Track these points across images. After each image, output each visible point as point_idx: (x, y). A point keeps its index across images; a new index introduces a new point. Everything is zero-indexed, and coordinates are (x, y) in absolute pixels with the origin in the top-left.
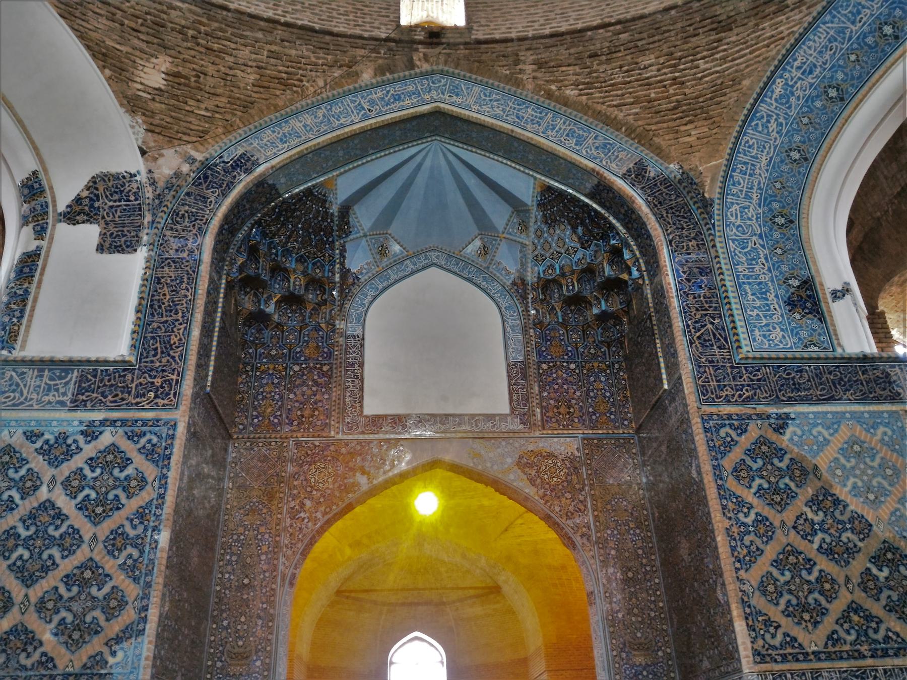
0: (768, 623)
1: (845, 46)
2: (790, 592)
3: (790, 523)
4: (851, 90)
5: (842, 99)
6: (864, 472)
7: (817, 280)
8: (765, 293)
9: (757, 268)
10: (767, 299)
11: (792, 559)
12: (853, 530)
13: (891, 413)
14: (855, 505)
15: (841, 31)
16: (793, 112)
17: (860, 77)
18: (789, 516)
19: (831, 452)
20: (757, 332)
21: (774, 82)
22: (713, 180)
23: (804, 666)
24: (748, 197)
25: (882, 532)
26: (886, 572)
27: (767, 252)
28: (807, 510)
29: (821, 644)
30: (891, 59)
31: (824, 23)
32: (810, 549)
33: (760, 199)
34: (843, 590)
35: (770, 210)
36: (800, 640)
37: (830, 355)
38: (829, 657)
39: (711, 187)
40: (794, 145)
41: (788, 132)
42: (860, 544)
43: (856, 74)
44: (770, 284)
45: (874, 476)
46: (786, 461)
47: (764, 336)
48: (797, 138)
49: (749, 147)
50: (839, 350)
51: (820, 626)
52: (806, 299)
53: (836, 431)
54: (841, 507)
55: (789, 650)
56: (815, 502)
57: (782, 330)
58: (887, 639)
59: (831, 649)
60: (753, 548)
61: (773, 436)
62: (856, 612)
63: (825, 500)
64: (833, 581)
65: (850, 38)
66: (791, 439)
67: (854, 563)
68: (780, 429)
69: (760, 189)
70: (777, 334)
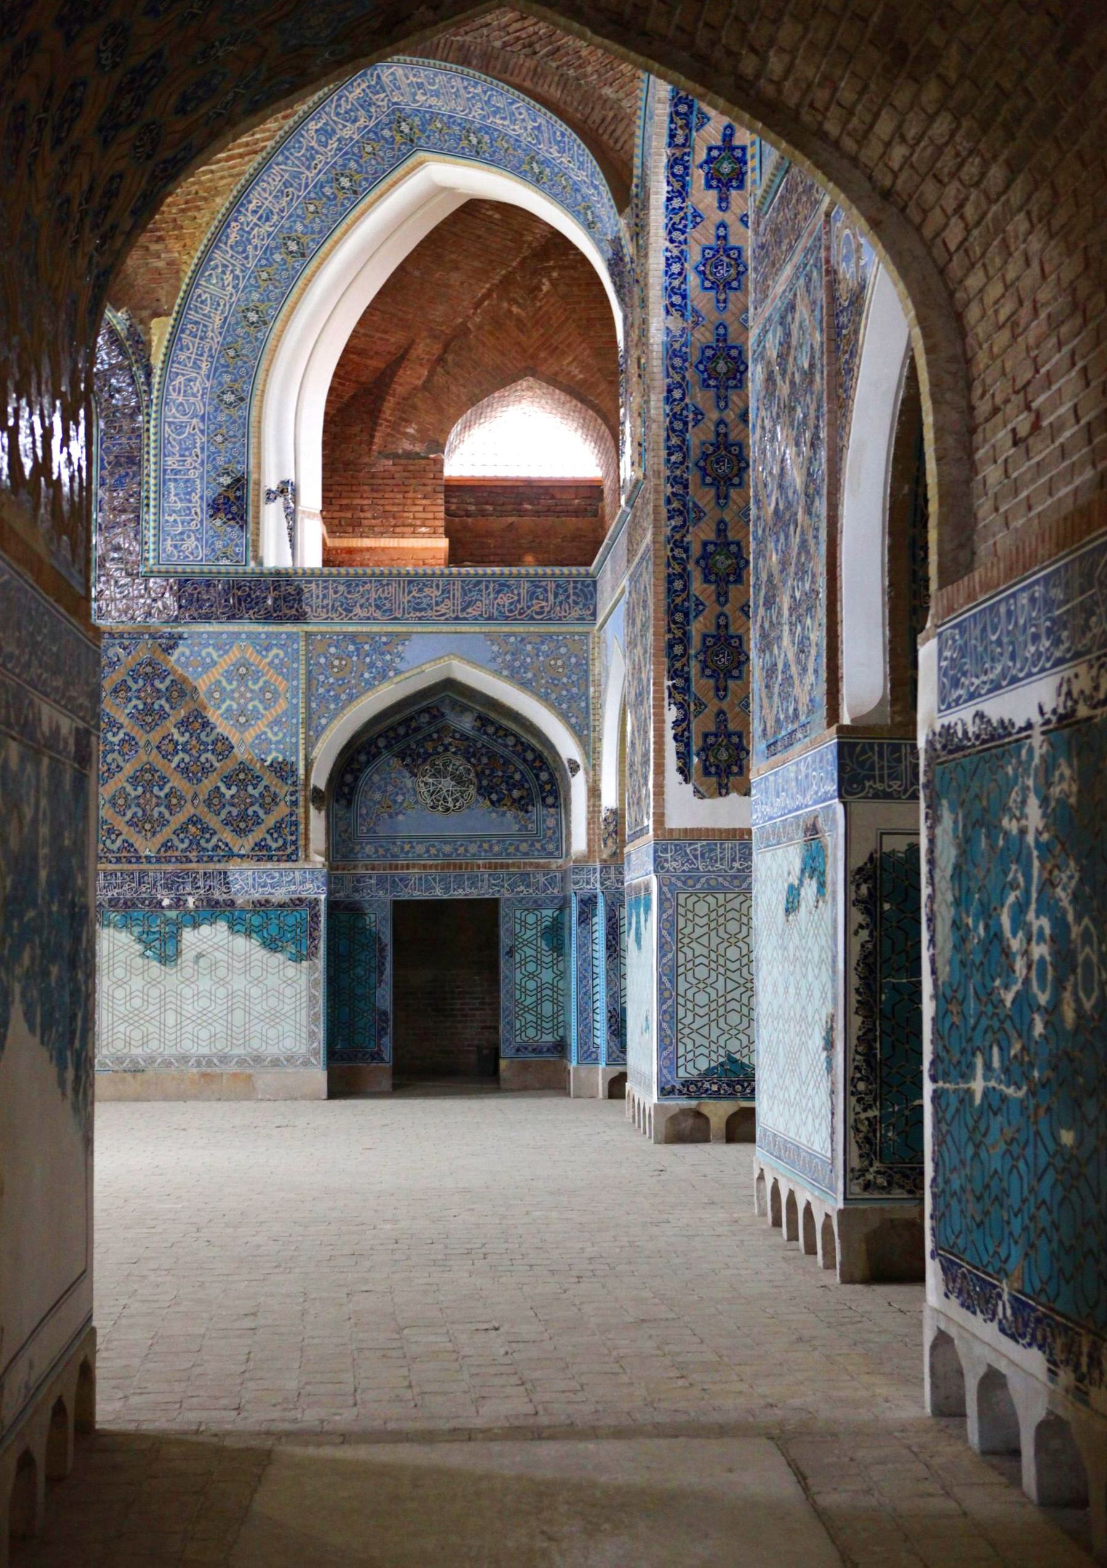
0: (110, 831)
1: (303, 194)
2: (138, 805)
3: (154, 744)
4: (312, 245)
5: (303, 255)
6: (242, 695)
7: (253, 477)
8: (189, 494)
9: (189, 460)
10: (190, 501)
11: (148, 776)
12: (213, 751)
13: (289, 635)
14: (223, 728)
15: (296, 176)
16: (251, 264)
17: (320, 232)
18: (155, 737)
19: (216, 674)
20: (169, 542)
21: (228, 226)
22: (160, 339)
23: (135, 866)
24: (196, 366)
25: (240, 753)
26: (234, 790)
27: (204, 439)
28: (174, 731)
29: (155, 850)
30: (351, 217)
31: (278, 164)
32: (168, 767)
33: (209, 370)
34: (189, 805)
35: (220, 384)
36: (136, 846)
37: (240, 569)
38: (158, 861)
39: (158, 345)
40: (251, 305)
41: (245, 287)
42: (217, 765)
43: (317, 228)
44: (198, 482)
45: (251, 699)
46: (168, 682)
47: (176, 546)
48: (255, 296)
49: (202, 302)
50: (252, 564)
51: (158, 836)
52: (234, 503)
53: (226, 652)
54: (208, 729)
55: (125, 854)
56: (184, 724)
57: (197, 539)
58: (217, 846)
59: (162, 854)
60: (113, 766)
61: (160, 656)
62: (194, 824)
63: (196, 722)
64: (181, 798)
65: (307, 186)
66: (178, 660)
67: (206, 781)
68: (168, 649)
69: (211, 356)
70: (191, 543)
